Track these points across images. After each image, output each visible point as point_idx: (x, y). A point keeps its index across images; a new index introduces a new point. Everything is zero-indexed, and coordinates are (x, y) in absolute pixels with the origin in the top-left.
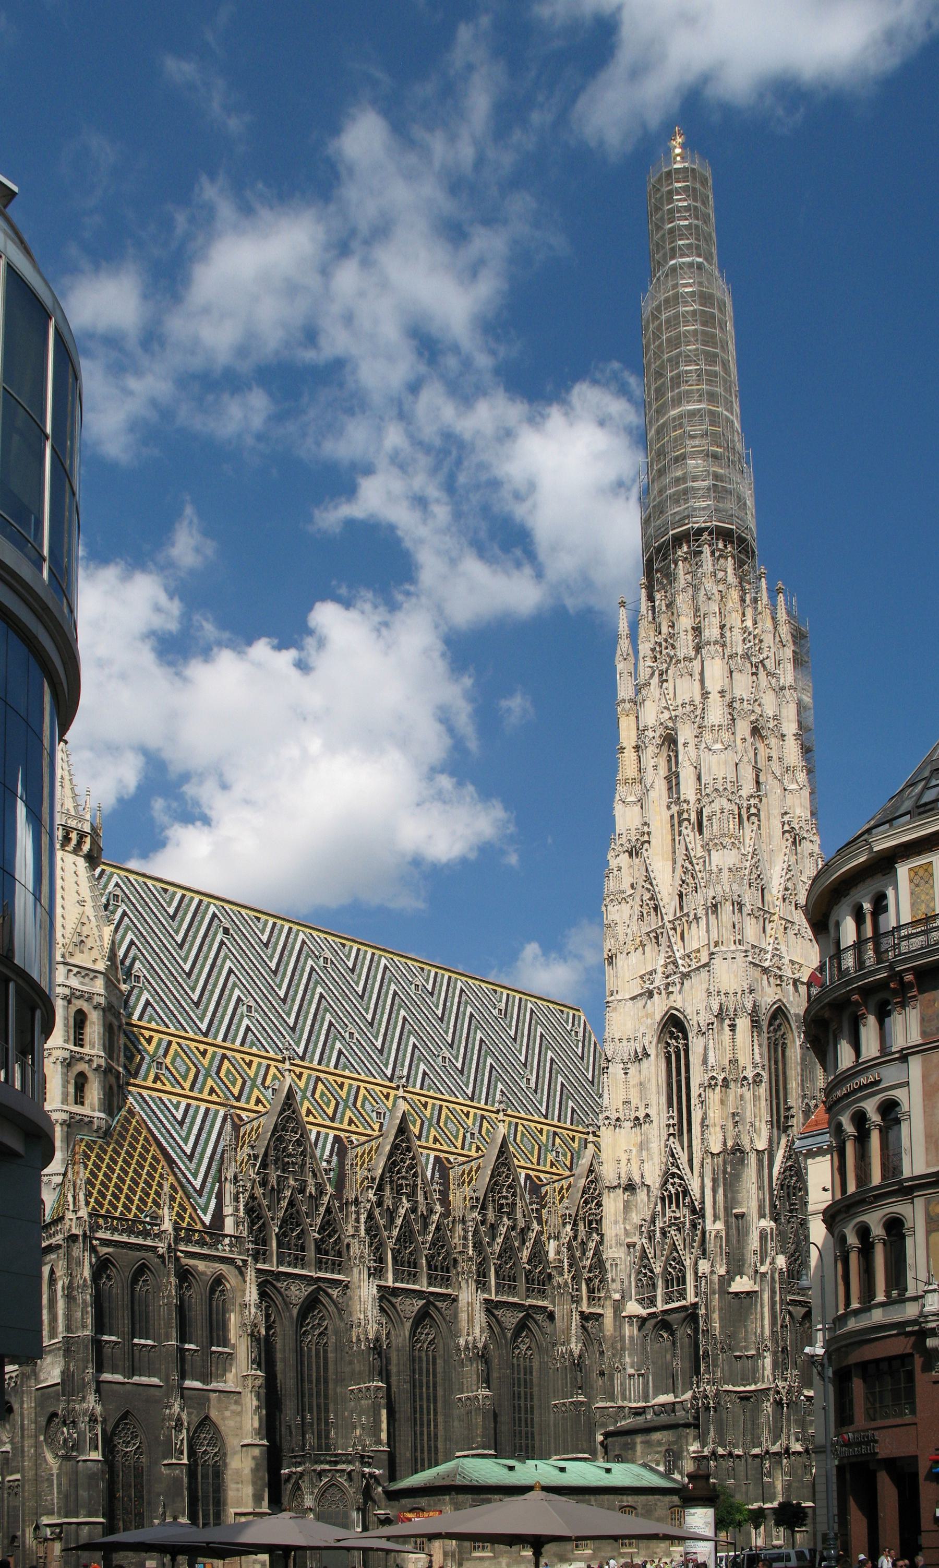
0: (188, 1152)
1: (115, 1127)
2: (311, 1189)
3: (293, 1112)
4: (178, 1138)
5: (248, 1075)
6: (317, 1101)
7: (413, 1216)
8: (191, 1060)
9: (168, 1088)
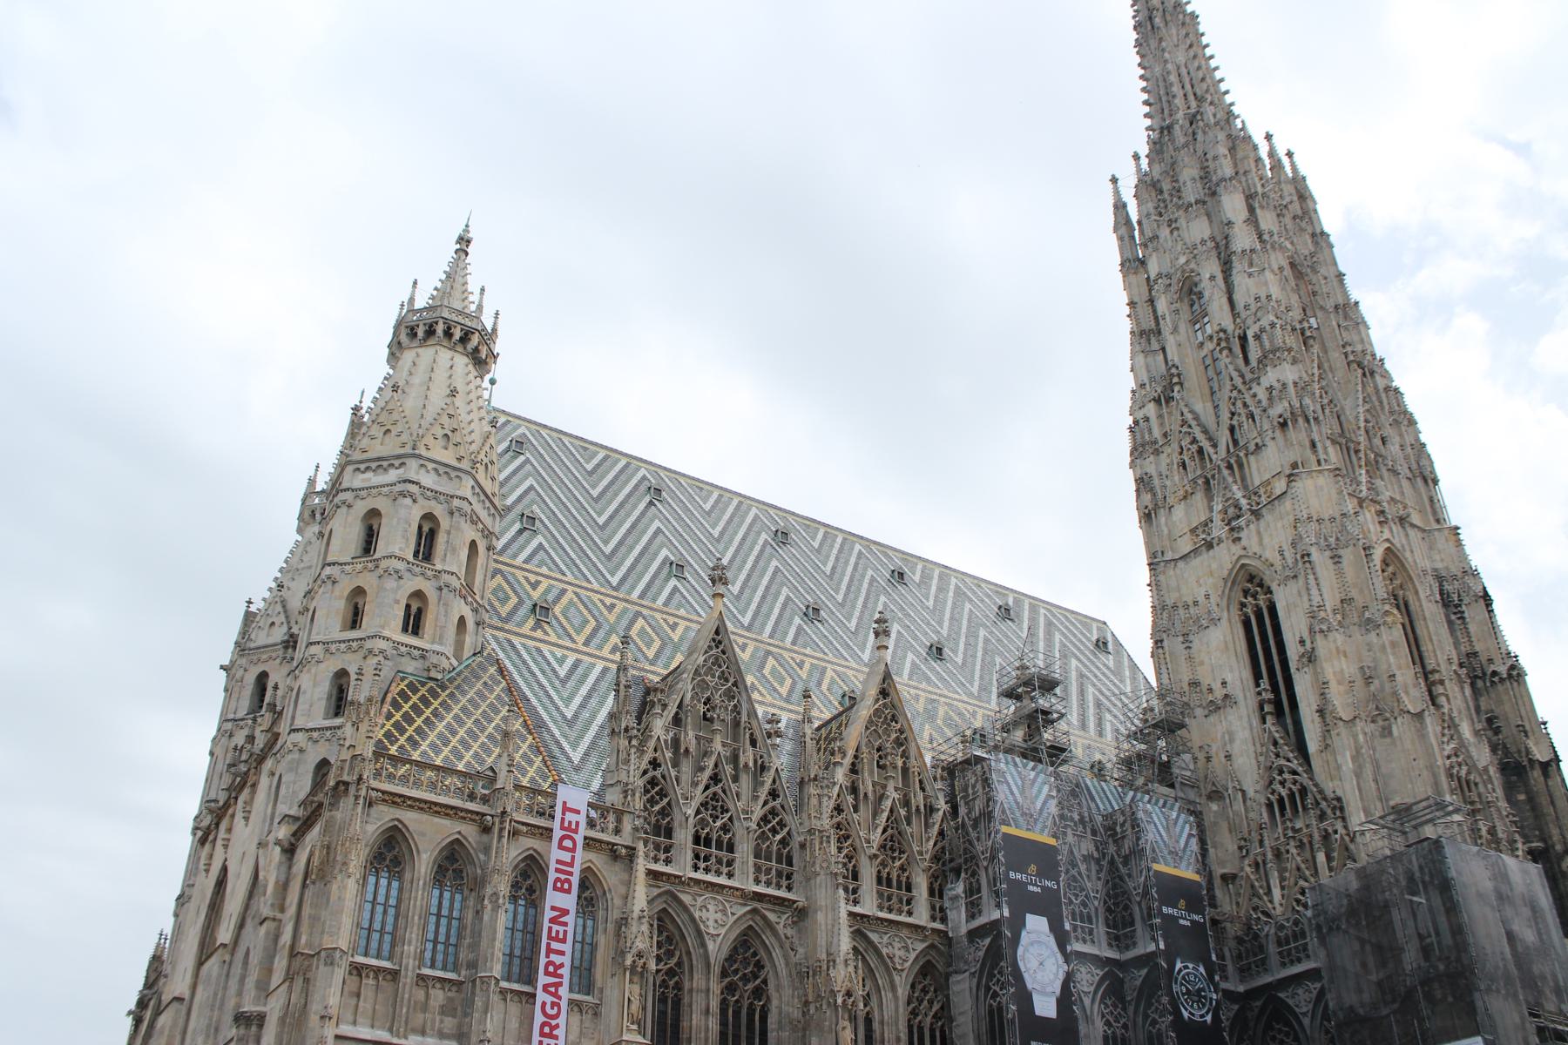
0: (569, 715)
1: (461, 671)
2: (748, 756)
3: (723, 652)
4: (555, 697)
5: (670, 638)
6: (764, 676)
7: (903, 812)
8: (590, 612)
9: (553, 638)
